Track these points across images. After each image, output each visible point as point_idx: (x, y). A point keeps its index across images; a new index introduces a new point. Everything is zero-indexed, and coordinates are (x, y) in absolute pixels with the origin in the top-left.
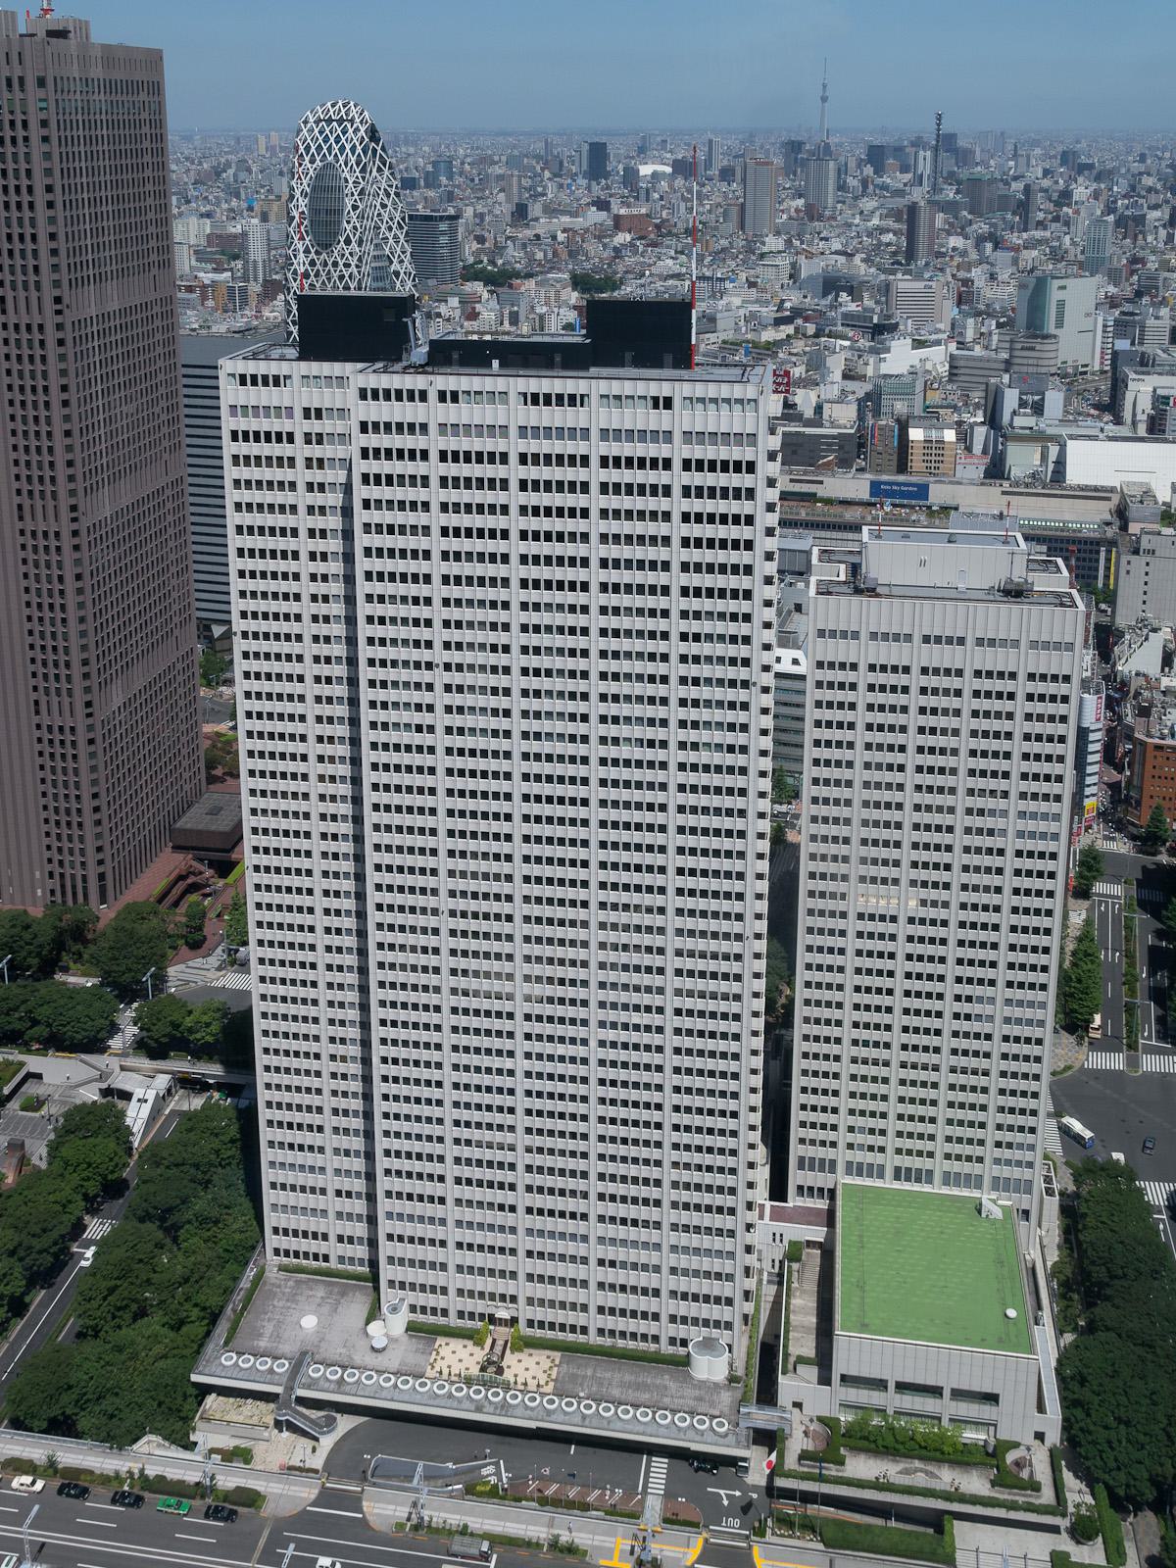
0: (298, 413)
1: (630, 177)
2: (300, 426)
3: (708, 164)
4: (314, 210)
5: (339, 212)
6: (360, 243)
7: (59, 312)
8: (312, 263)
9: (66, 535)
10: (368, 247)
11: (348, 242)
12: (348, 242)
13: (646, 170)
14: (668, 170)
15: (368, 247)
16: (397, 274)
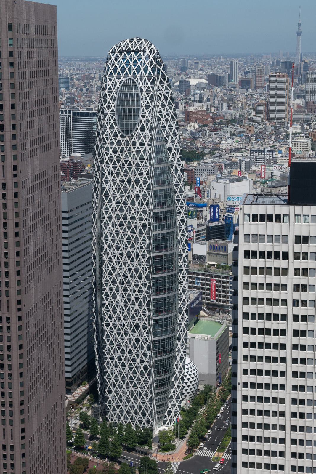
0: (292, 239)
1: (185, 87)
2: (292, 248)
3: (230, 77)
4: (121, 110)
5: (136, 110)
6: (151, 130)
7: (15, 176)
8: (119, 143)
9: (14, 319)
10: (154, 132)
11: (143, 129)
12: (143, 129)
13: (193, 82)
14: (205, 81)
15: (154, 132)
16: (170, 149)
